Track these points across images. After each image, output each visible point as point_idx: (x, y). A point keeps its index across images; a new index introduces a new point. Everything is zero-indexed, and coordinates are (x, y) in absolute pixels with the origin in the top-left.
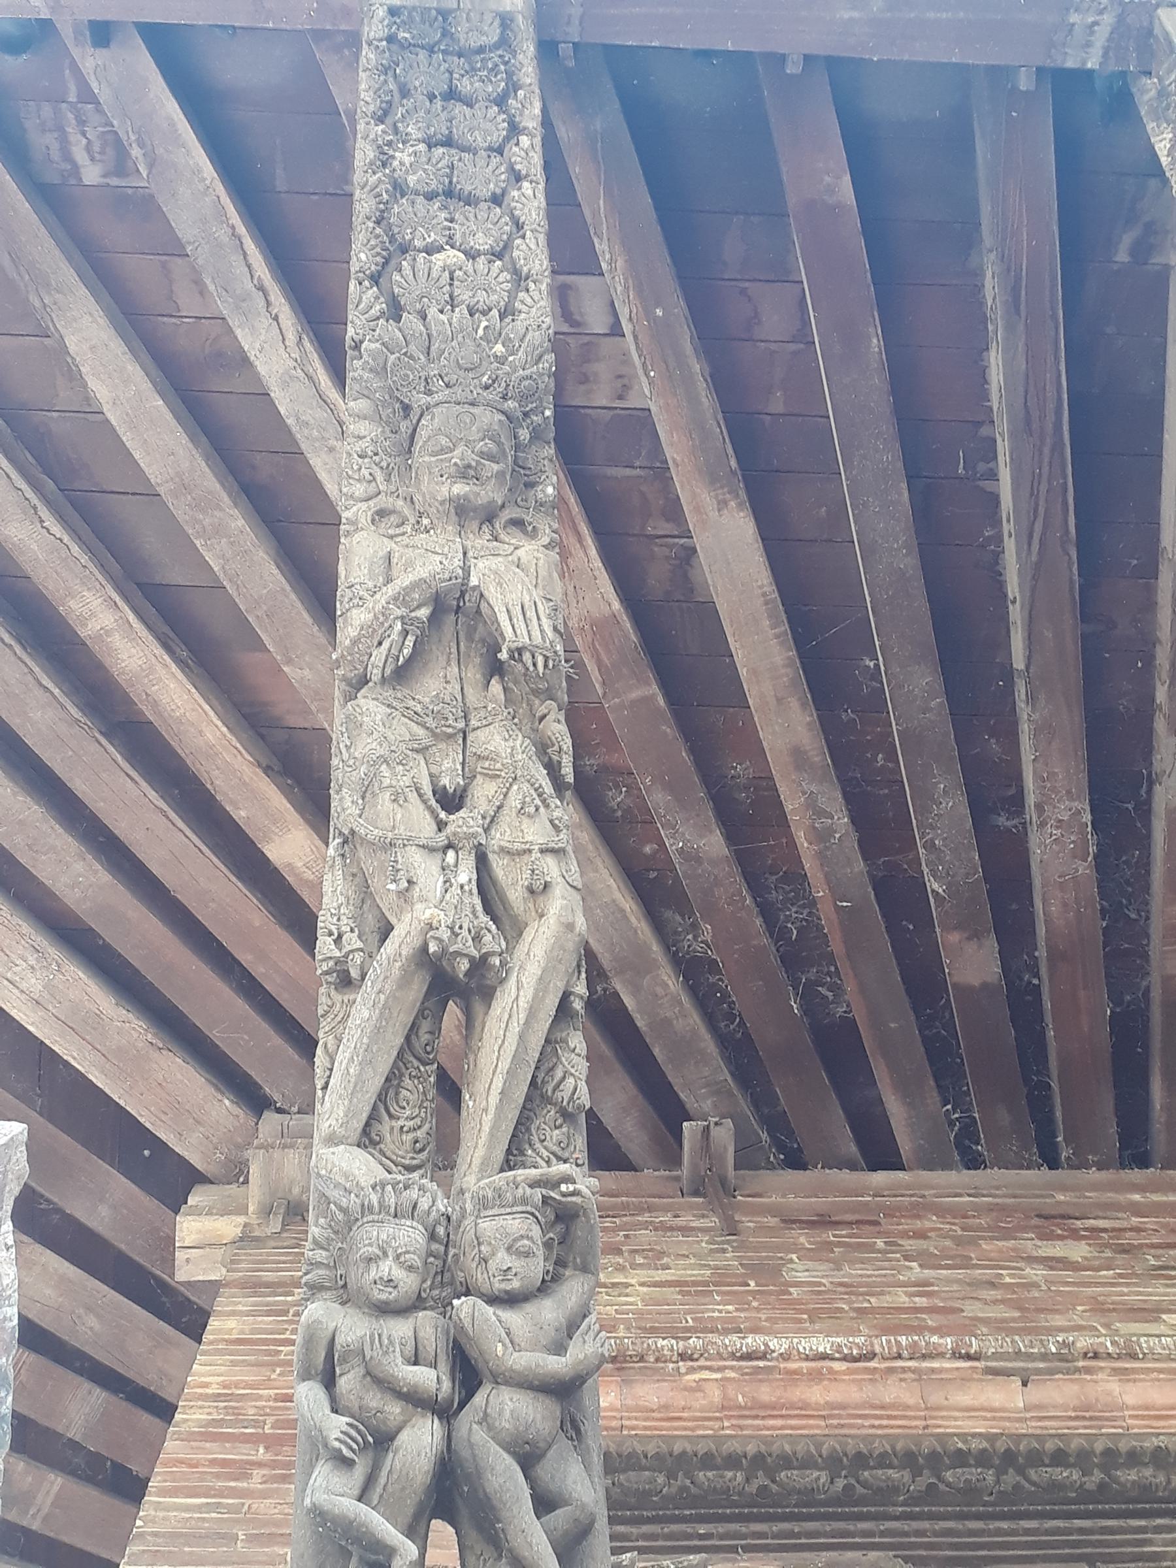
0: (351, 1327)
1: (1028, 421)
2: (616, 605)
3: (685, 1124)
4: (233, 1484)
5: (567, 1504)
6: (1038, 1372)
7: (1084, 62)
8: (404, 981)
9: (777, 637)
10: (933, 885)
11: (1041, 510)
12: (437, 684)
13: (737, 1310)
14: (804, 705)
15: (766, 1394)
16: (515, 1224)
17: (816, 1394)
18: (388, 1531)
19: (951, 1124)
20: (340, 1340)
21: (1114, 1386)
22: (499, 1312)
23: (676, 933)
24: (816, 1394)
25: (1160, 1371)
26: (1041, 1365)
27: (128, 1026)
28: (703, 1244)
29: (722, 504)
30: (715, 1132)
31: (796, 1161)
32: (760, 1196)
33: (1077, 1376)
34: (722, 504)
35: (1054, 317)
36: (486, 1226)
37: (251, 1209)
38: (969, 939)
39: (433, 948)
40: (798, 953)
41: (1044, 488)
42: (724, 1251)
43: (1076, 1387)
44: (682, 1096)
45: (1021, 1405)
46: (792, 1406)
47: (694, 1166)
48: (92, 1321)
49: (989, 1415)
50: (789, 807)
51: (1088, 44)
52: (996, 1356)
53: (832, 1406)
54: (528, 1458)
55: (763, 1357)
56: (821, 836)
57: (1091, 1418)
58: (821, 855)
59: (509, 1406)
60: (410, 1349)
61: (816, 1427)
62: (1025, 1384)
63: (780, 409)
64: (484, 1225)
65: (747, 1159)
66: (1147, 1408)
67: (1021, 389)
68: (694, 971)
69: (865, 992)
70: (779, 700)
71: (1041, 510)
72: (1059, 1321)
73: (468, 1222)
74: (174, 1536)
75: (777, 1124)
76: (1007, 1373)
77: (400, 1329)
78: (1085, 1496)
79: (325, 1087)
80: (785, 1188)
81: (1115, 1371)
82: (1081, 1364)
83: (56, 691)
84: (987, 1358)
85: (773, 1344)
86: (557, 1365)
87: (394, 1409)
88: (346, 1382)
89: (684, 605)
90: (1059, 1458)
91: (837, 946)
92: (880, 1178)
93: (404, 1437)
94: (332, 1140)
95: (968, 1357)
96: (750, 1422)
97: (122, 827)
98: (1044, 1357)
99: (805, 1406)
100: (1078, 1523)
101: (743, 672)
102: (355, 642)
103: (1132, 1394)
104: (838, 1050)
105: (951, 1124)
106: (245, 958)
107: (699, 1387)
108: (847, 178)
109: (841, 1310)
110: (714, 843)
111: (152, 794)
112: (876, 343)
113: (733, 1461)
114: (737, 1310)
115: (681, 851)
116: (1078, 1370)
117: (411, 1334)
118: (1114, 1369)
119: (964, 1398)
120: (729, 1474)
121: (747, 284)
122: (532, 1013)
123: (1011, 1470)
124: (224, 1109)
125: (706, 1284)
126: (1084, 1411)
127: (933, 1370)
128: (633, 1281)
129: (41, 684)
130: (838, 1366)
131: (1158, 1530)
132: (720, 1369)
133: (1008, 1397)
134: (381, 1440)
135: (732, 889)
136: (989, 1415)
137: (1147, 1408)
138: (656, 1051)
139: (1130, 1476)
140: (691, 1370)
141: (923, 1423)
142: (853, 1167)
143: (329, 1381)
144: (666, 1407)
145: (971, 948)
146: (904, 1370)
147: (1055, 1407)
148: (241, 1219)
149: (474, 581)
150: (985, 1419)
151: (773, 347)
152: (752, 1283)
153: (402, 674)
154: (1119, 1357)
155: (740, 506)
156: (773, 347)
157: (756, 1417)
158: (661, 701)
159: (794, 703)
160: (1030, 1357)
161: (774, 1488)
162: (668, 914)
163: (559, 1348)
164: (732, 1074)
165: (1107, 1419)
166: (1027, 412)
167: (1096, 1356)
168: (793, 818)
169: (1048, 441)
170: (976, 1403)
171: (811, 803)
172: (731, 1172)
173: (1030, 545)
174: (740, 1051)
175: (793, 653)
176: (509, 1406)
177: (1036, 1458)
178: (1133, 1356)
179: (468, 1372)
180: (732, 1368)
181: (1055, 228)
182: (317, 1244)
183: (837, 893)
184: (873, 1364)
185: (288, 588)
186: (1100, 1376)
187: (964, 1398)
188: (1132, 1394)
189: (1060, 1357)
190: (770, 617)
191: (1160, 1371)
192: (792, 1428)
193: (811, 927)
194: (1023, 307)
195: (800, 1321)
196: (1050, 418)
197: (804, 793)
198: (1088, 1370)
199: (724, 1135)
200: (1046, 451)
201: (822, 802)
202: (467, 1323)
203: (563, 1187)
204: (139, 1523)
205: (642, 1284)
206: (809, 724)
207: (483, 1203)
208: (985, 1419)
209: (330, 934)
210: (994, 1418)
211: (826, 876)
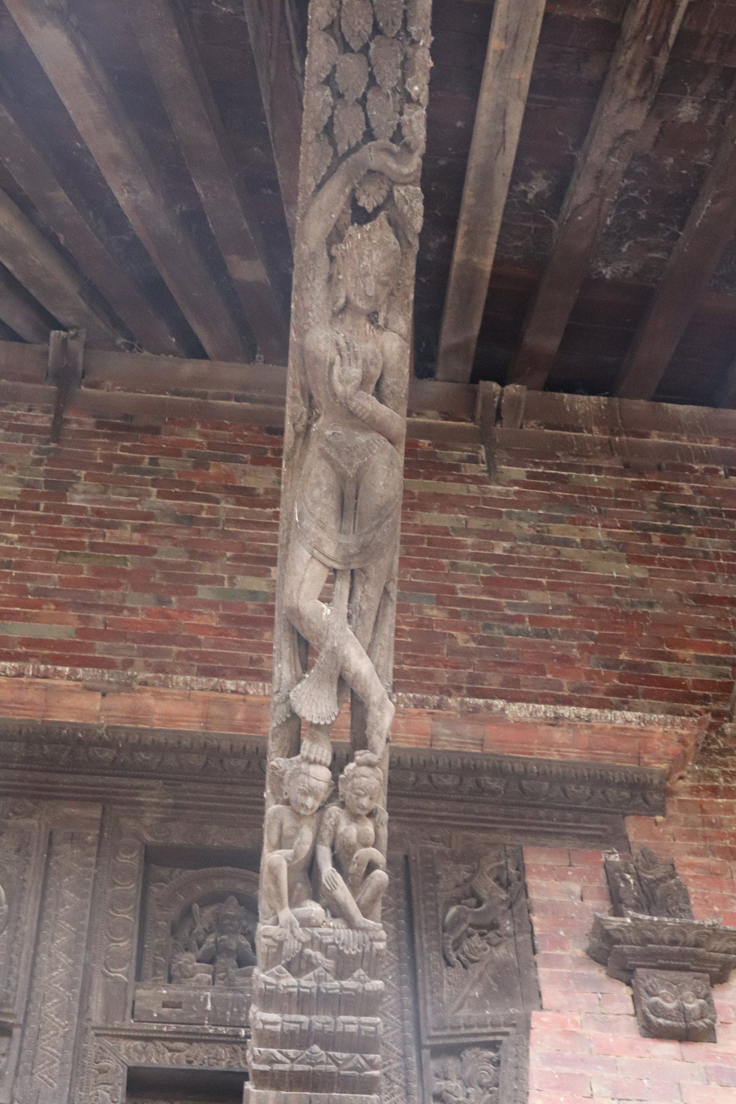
3: (53, 333)
13: (20, 540)
21: (152, 702)
25: (179, 695)
28: (31, 453)
43: (130, 701)
45: (98, 708)
62: (104, 695)
90: (106, 745)
92: (189, 368)
114: (20, 540)
127: (54, 686)
133: (93, 703)
146: (38, 684)
152: (42, 506)
167: (146, 684)
184: (23, 679)
187: (68, 702)
195: (49, 556)
198: (139, 691)
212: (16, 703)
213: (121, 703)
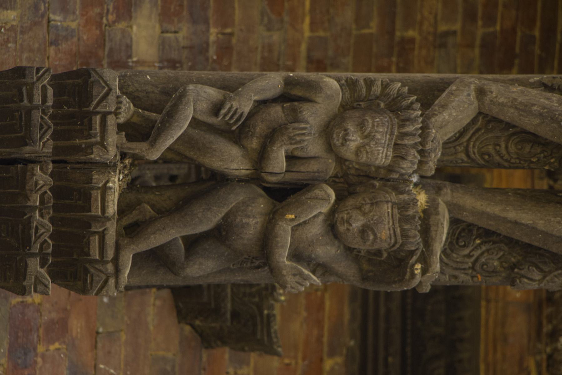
0: (314, 116)
22: (321, 218)
36: (387, 208)
54: (221, 234)
60: (298, 153)
64: (387, 208)
73: (393, 197)
77: (313, 146)
86: (282, 257)
87: (254, 144)
88: (277, 112)
93: (235, 151)
117: (312, 154)
134: (236, 134)
143: (283, 98)
176: (252, 221)
179: (284, 194)
202: (310, 195)
203: (418, 266)
207: (403, 207)
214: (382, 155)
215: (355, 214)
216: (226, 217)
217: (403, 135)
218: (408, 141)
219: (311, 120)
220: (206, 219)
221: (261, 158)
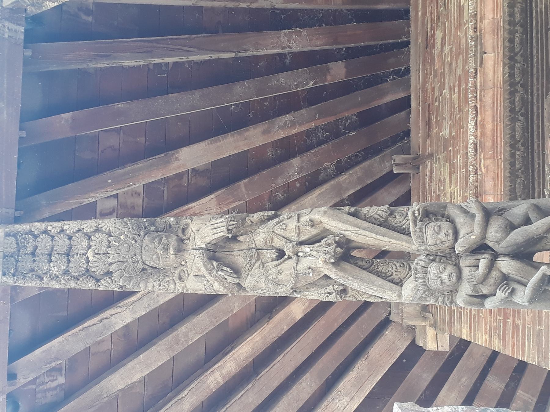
0: (466, 289)
1: (147, 52)
2: (212, 196)
3: (394, 172)
4: (521, 330)
5: (527, 213)
6: (481, 48)
7: (22, 32)
8: (344, 270)
9: (223, 140)
10: (311, 85)
11: (179, 47)
12: (240, 258)
14: (247, 130)
15: (489, 144)
16: (429, 231)
17: (489, 126)
18: (537, 276)
19: (394, 79)
20: (470, 293)
21: (486, 22)
22: (460, 237)
23: (327, 175)
24: (489, 126)
25: (481, 5)
26: (479, 47)
27: (360, 367)
29: (177, 159)
30: (397, 162)
31: (407, 133)
32: (419, 146)
33: (483, 35)
34: (177, 159)
35: (111, 43)
37: (424, 324)
38: (329, 73)
39: (332, 260)
40: (334, 132)
41: (171, 46)
42: (439, 158)
43: (487, 35)
44: (384, 173)
46: (494, 134)
47: (409, 169)
48: (463, 380)
49: (496, 66)
50: (283, 136)
51: (16, 31)
52: (476, 63)
53: (493, 121)
54: (511, 227)
55: (476, 145)
56: (293, 124)
57: (498, 30)
58: (300, 125)
59: (493, 234)
61: (501, 126)
62: (485, 53)
63: (143, 139)
64: (430, 242)
65: (406, 150)
66: (494, 10)
67: (137, 54)
68: (340, 169)
69: (348, 109)
70: (246, 139)
71: (179, 47)
72: (463, 41)
74: (539, 351)
75: (394, 140)
76: (482, 59)
77: (466, 272)
78: (525, 32)
79: (381, 298)
80: (417, 137)
81: (481, 21)
82: (478, 33)
83: (242, 392)
84: (476, 66)
85: (471, 141)
86: (479, 217)
87: (494, 274)
88: (485, 290)
89: (212, 172)
90: (511, 41)
91: (332, 119)
92: (413, 104)
93: (504, 271)
94: (400, 296)
95: (476, 73)
96: (499, 149)
97: (290, 369)
98: (476, 46)
99: (493, 130)
100: (534, 34)
101: (236, 152)
102: (225, 288)
103: (489, 15)
104: (368, 118)
105: (394, 79)
106: (336, 326)
107: (487, 167)
108: (63, 115)
109: (459, 117)
110: (296, 162)
111: (279, 359)
112: (120, 105)
113: (513, 155)
115: (299, 174)
116: (481, 34)
117: (468, 268)
118: (480, 22)
119: (490, 74)
120: (517, 156)
121: (100, 150)
122: (355, 226)
123: (516, 58)
124: (389, 333)
125: (450, 165)
126: (495, 32)
127: (481, 85)
128: (449, 190)
129: (240, 398)
130: (479, 119)
131: (537, 6)
132: (480, 160)
133: (490, 59)
134: (505, 279)
135: (312, 156)
136: (496, 66)
137: (494, 10)
138: (369, 182)
139: (518, 16)
140: (481, 170)
141: (499, 89)
142: (409, 113)
143: (484, 297)
144: (494, 179)
145: (332, 72)
147: (494, 43)
148: (428, 327)
149: (204, 246)
150: (498, 67)
151: (122, 141)
152: (450, 148)
153: (236, 271)
154: (476, 20)
155: (177, 153)
156: (122, 141)
157: (497, 147)
158: (246, 180)
159: (247, 134)
160: (476, 51)
161: (522, 141)
162: (321, 178)
163: (473, 216)
164: (377, 156)
165: (498, 24)
166: (145, 52)
167: (476, 28)
168: (287, 134)
169: (155, 45)
170: (492, 70)
171: (282, 128)
172: (411, 156)
173: (191, 51)
174: (369, 153)
175: (229, 134)
176: (493, 234)
177: (512, 49)
178: (476, 15)
179: (482, 248)
180: (480, 156)
181: (80, 42)
182: (436, 301)
183: (313, 119)
184: (479, 106)
185: (206, 311)
186: (483, 26)
187: (490, 74)
188: (489, 15)
189: (476, 41)
190: (216, 142)
191: (481, 5)
192: (501, 134)
193: (325, 128)
194: (107, 54)
195: (463, 132)
196: (146, 44)
197: (278, 130)
198: (481, 31)
199: (398, 158)
200: (158, 45)
201: (281, 124)
202: (464, 248)
203: (416, 215)
204: (534, 363)
205: (451, 187)
206: (254, 129)
207: (422, 243)
208: (498, 67)
209: (328, 296)
210: (498, 64)
211: (307, 123)
212: (494, 106)
213: (489, 41)
214: (433, 268)
215: (444, 240)
216: (508, 234)
217: (423, 278)
218: (421, 275)
219: (468, 286)
220: (518, 235)
221: (491, 266)
